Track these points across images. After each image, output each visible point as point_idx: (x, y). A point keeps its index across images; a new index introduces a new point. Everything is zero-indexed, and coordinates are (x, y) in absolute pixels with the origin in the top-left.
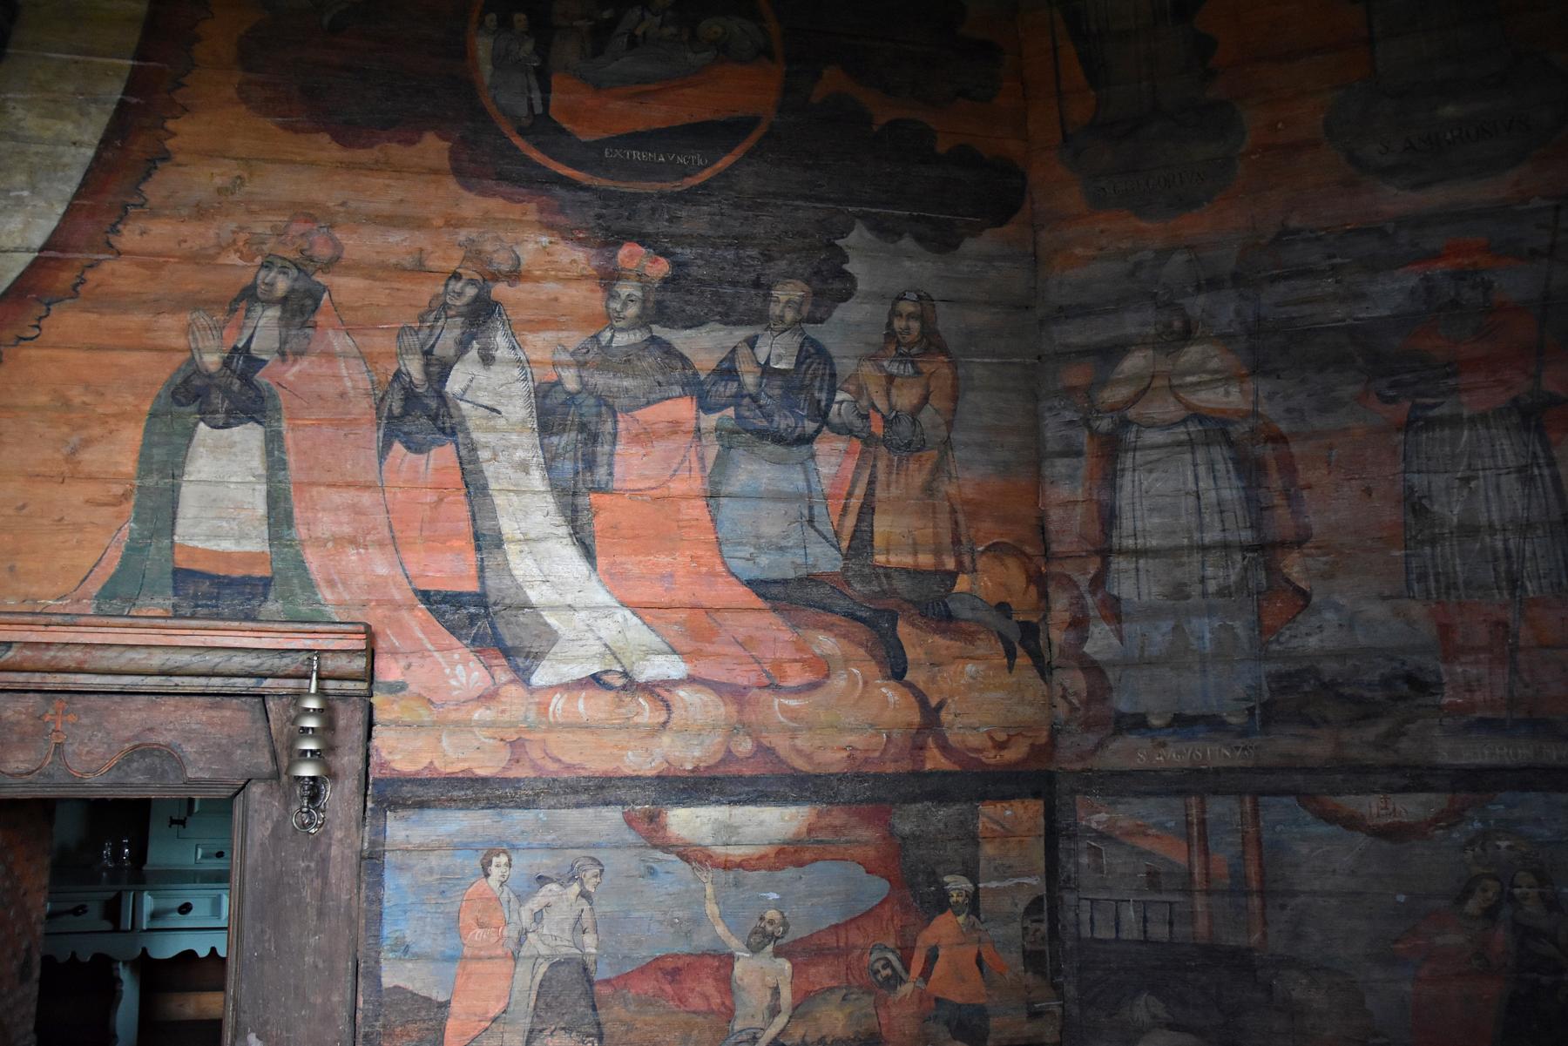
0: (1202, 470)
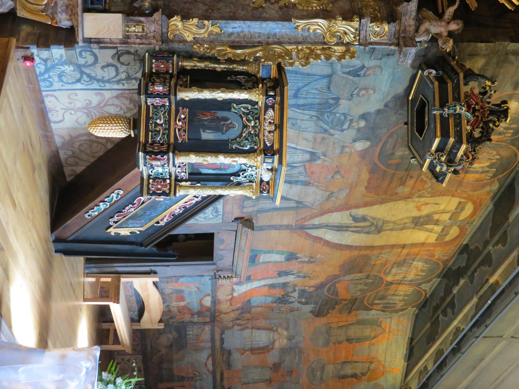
0: (265, 342)
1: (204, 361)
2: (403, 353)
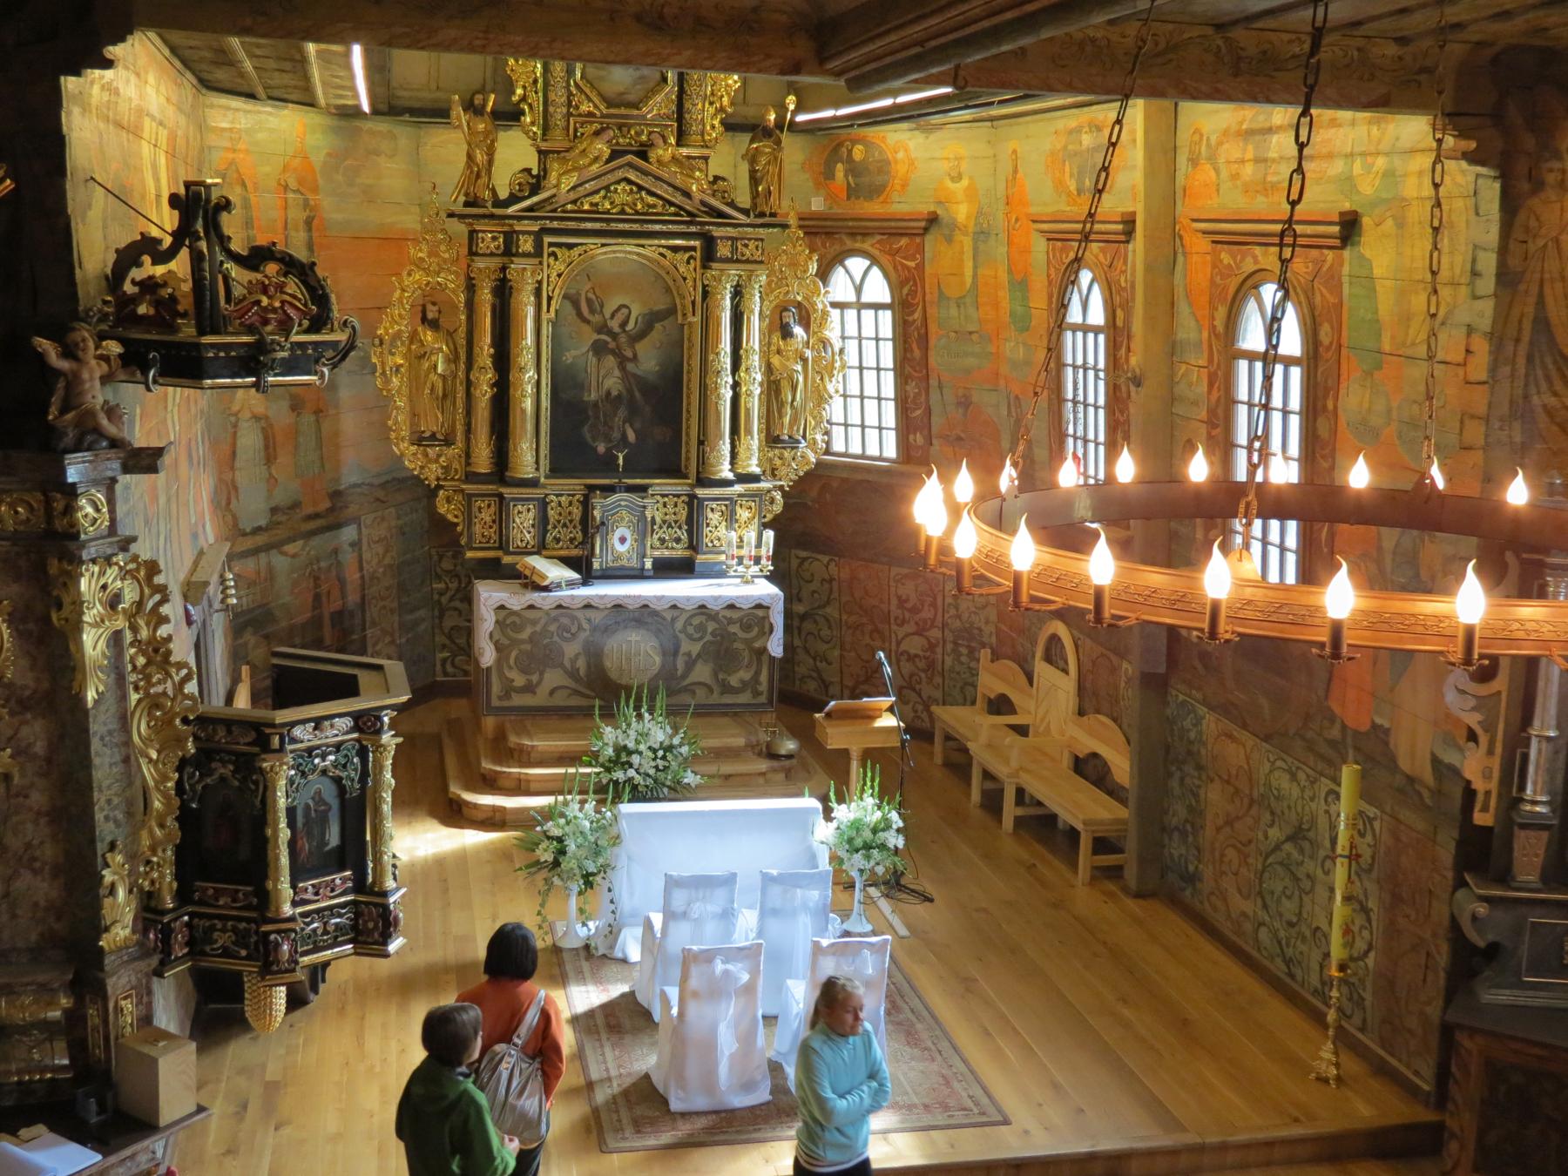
1: (289, 559)
2: (270, 114)
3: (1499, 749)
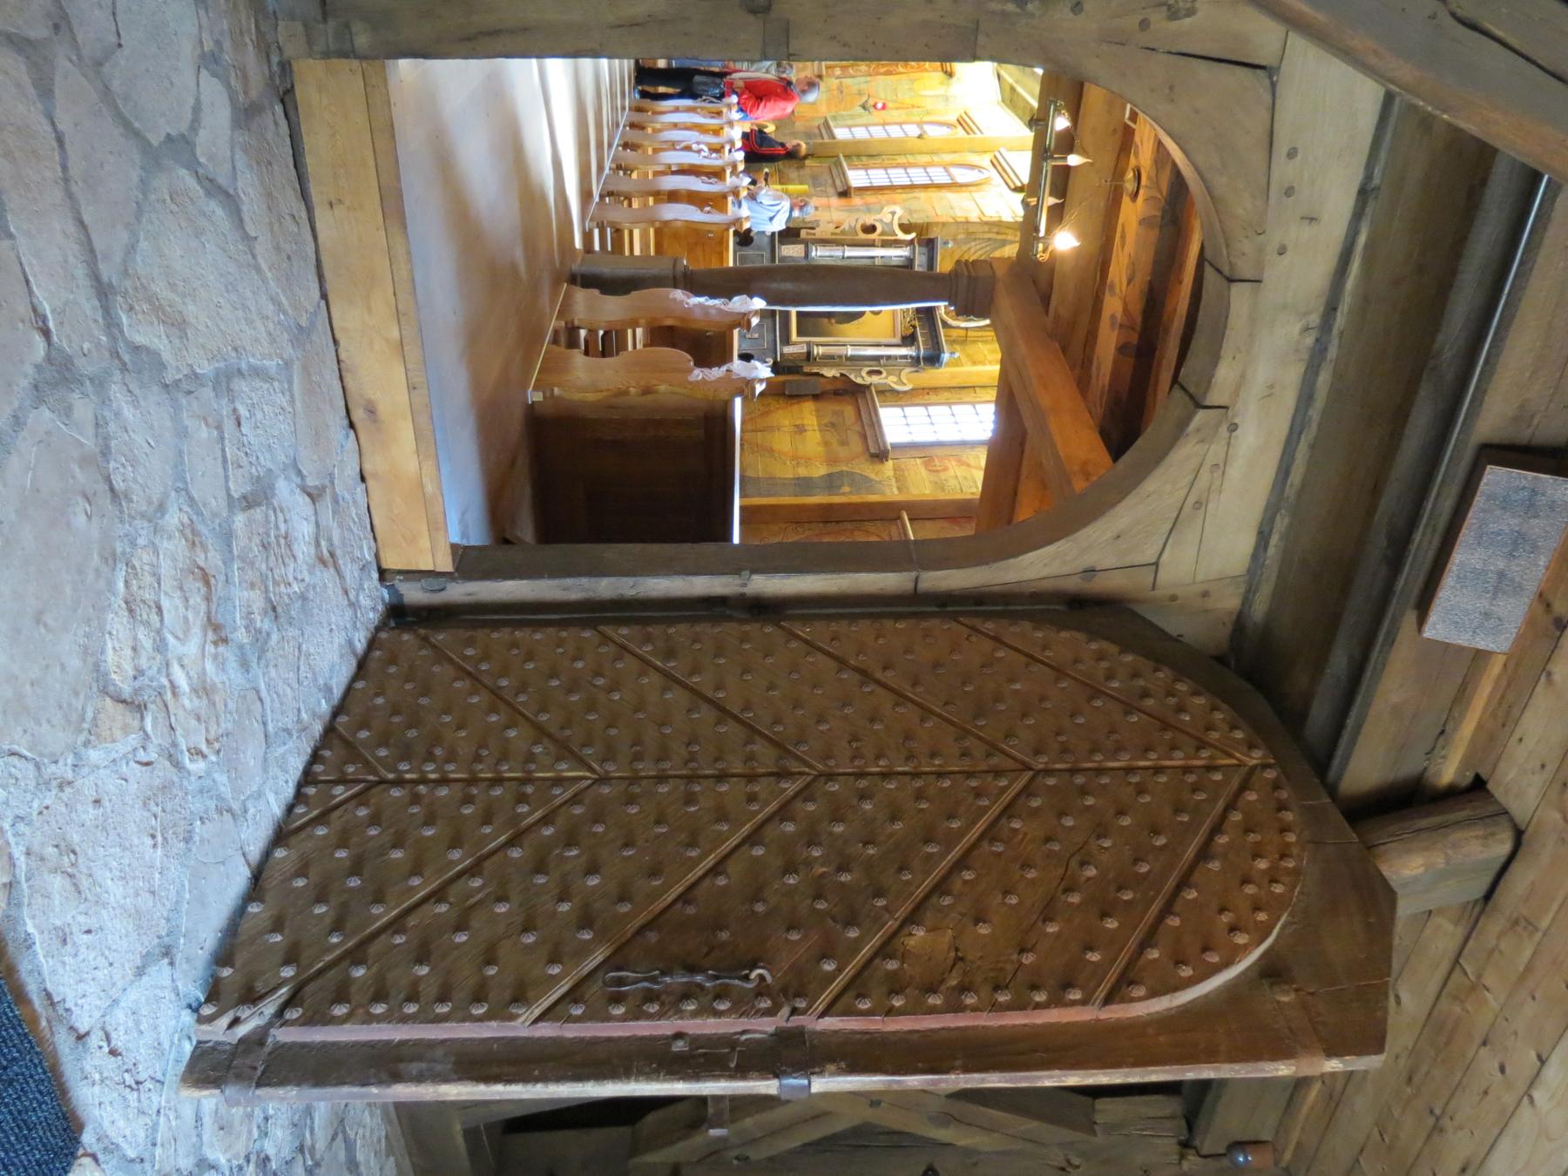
3: (833, 237)
